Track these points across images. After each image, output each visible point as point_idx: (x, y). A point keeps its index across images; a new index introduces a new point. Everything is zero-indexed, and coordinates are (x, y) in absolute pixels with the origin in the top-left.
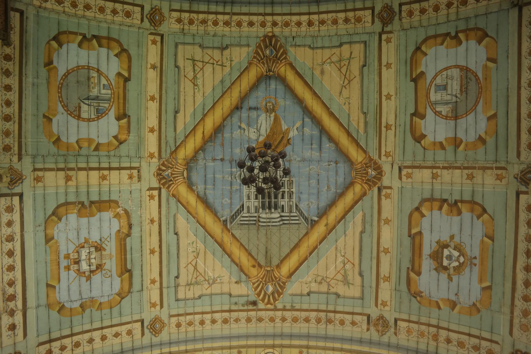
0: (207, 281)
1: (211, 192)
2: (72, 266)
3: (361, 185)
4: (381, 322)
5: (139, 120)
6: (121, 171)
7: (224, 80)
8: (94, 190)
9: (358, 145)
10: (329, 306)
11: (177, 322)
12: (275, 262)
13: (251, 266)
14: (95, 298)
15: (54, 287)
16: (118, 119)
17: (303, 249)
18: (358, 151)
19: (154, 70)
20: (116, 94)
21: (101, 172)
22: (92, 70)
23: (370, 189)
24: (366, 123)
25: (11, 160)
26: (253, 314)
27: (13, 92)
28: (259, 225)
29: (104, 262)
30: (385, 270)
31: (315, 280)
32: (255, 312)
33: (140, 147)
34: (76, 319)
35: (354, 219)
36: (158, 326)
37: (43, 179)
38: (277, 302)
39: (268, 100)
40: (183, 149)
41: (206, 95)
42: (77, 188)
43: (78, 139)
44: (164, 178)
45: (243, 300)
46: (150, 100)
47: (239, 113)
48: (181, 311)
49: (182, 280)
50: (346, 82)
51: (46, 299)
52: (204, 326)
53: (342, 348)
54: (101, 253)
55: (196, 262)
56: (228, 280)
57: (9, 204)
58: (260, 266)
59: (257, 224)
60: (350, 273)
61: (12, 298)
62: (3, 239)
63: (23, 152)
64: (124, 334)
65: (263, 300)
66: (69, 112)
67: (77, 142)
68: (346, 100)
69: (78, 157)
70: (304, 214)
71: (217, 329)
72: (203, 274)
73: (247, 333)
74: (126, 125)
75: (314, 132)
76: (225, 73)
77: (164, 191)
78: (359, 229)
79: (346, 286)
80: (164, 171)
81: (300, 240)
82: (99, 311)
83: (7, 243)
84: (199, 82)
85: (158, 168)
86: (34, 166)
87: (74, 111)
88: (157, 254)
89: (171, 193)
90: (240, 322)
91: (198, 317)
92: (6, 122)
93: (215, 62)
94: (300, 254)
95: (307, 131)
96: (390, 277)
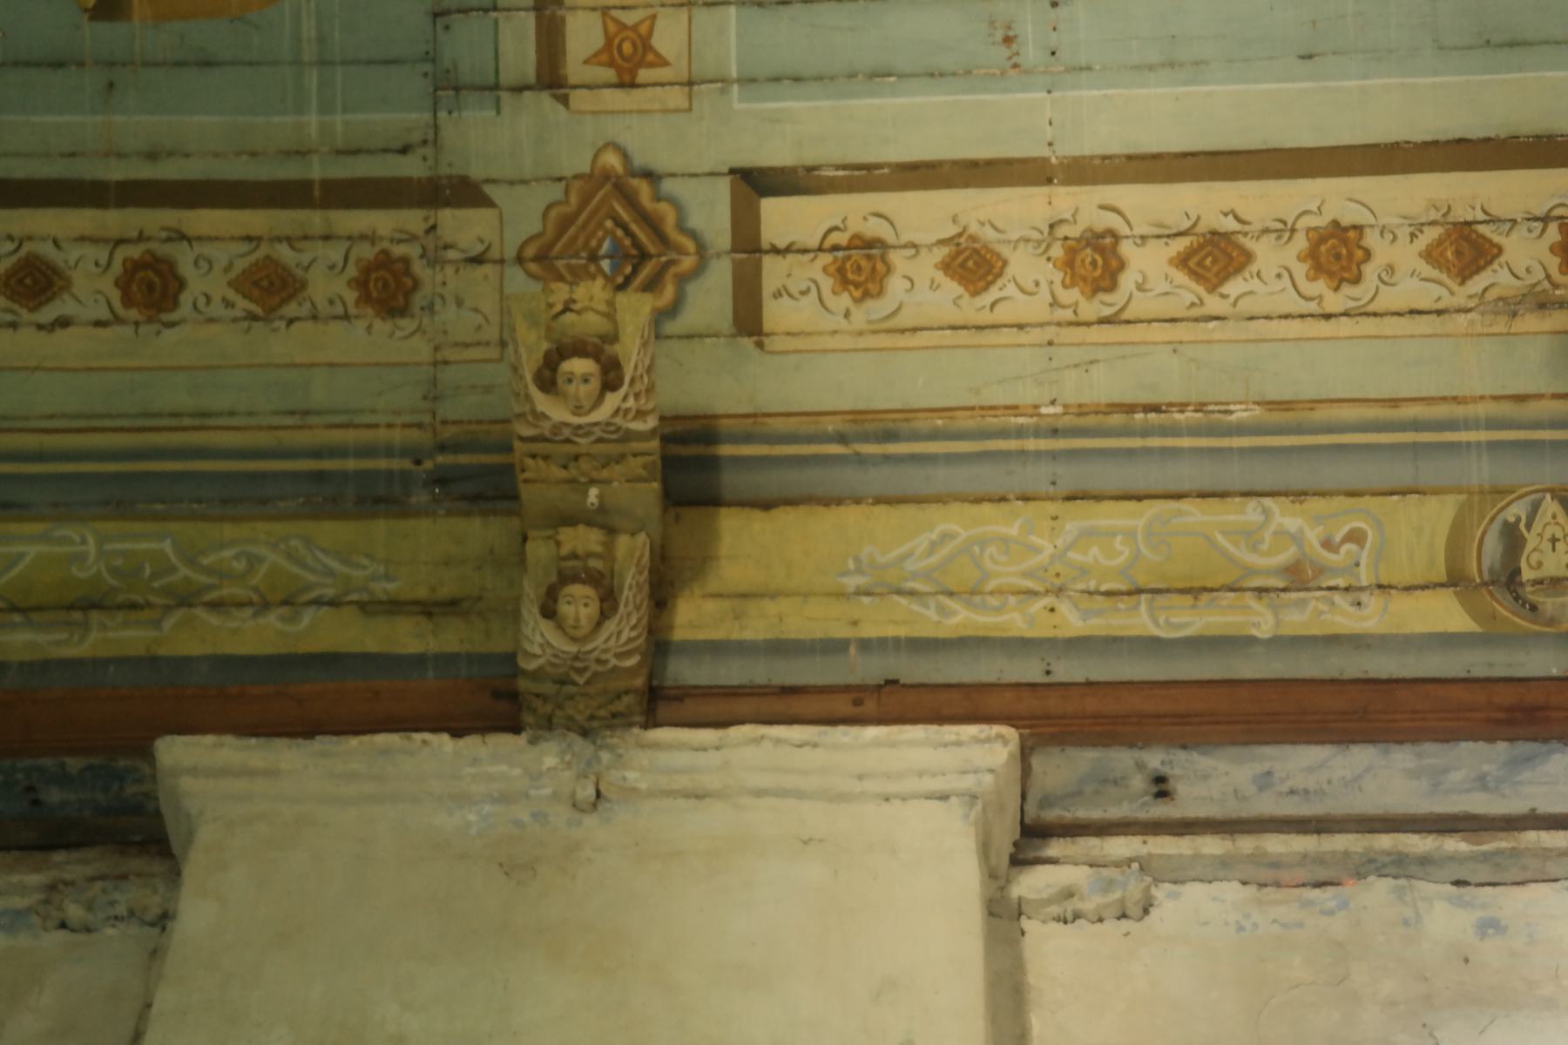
25: (477, 260)
37: (630, 18)
57: (816, 270)
63: (412, 167)
83: (1127, 280)
86: (519, 89)
92: (186, 298)
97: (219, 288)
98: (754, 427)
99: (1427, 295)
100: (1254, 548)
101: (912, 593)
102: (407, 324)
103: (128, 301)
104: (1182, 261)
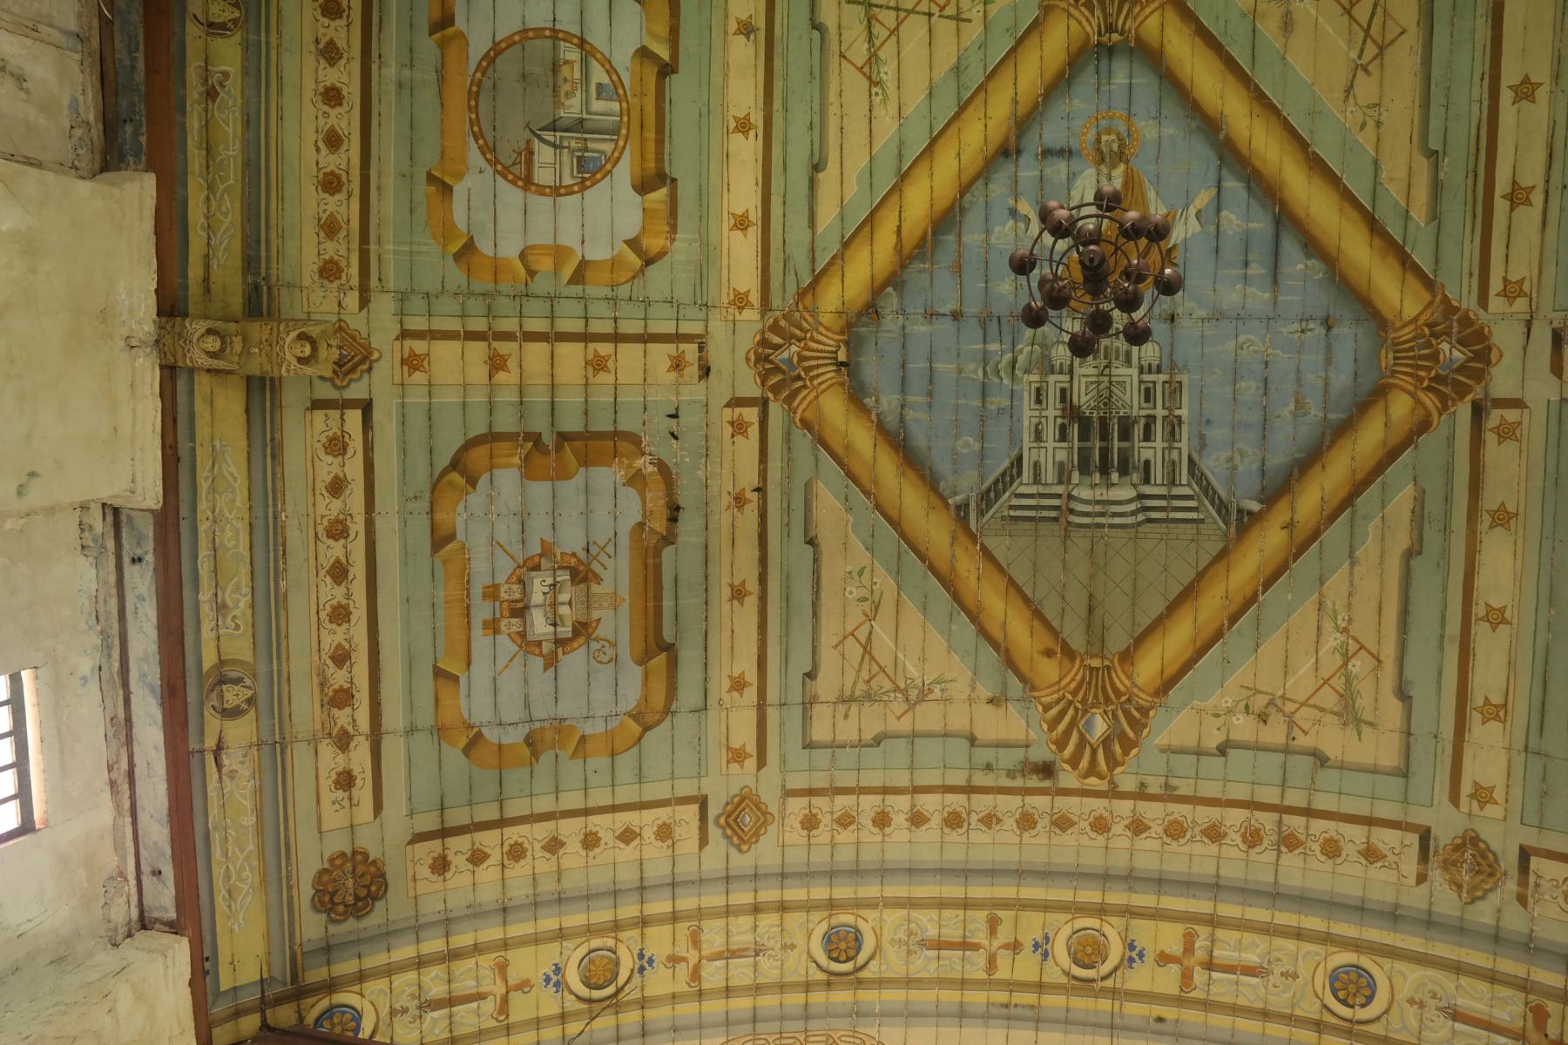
0: (901, 692)
1: (921, 415)
2: (504, 623)
3: (1413, 395)
4: (1468, 855)
5: (704, 192)
6: (649, 345)
7: (964, 63)
8: (570, 399)
9: (1405, 261)
10: (1289, 792)
11: (807, 811)
12: (1118, 641)
13: (1039, 652)
14: (567, 722)
15: (455, 679)
16: (642, 188)
17: (1211, 605)
18: (1403, 282)
19: (748, 38)
20: (635, 115)
21: (592, 346)
22: (565, 41)
23: (1445, 408)
24: (1436, 187)
25: (340, 304)
26: (1040, 802)
27: (346, 107)
28: (1068, 522)
29: (595, 615)
30: (1489, 678)
31: (1247, 707)
32: (1048, 798)
33: (705, 273)
34: (515, 778)
35: (1383, 507)
36: (748, 819)
37: (425, 363)
38: (1119, 770)
39: (1103, 123)
40: (836, 281)
41: (907, 112)
42: (521, 394)
43: (527, 248)
44: (777, 370)
45: (1012, 758)
46: (737, 130)
47: (1011, 168)
48: (820, 781)
49: (827, 684)
50: (1371, 50)
51: (432, 710)
52: (887, 830)
53: (1328, 933)
54: (588, 588)
55: (870, 633)
56: (967, 691)
57: (335, 430)
58: (1069, 654)
59: (1063, 520)
60: (1365, 687)
61: (343, 698)
62: (320, 529)
63: (374, 282)
64: (649, 833)
65: (1074, 762)
66: (499, 167)
67: (523, 256)
68: (1369, 112)
69: (524, 300)
70: (1215, 492)
71: (928, 844)
72: (890, 670)
73: (1020, 862)
74: (664, 208)
75: (1255, 225)
76: (966, 43)
77: (776, 410)
78: (1401, 541)
79: (1351, 732)
80: (777, 347)
81: (1201, 575)
82: (580, 762)
83: (331, 542)
84: (887, 73)
85: (758, 338)
86: (401, 322)
87: (514, 164)
88: (752, 602)
89: (798, 416)
90: (998, 828)
91: (870, 802)
92: (326, 196)
93: (935, 9)
94: (1199, 621)
95: (1232, 220)
96: (1505, 704)
97: (330, 209)
98: (277, 406)
99: (326, 646)
100: (233, 591)
101: (213, 466)
102: (316, 278)
103: (325, 174)
104: (338, 561)
